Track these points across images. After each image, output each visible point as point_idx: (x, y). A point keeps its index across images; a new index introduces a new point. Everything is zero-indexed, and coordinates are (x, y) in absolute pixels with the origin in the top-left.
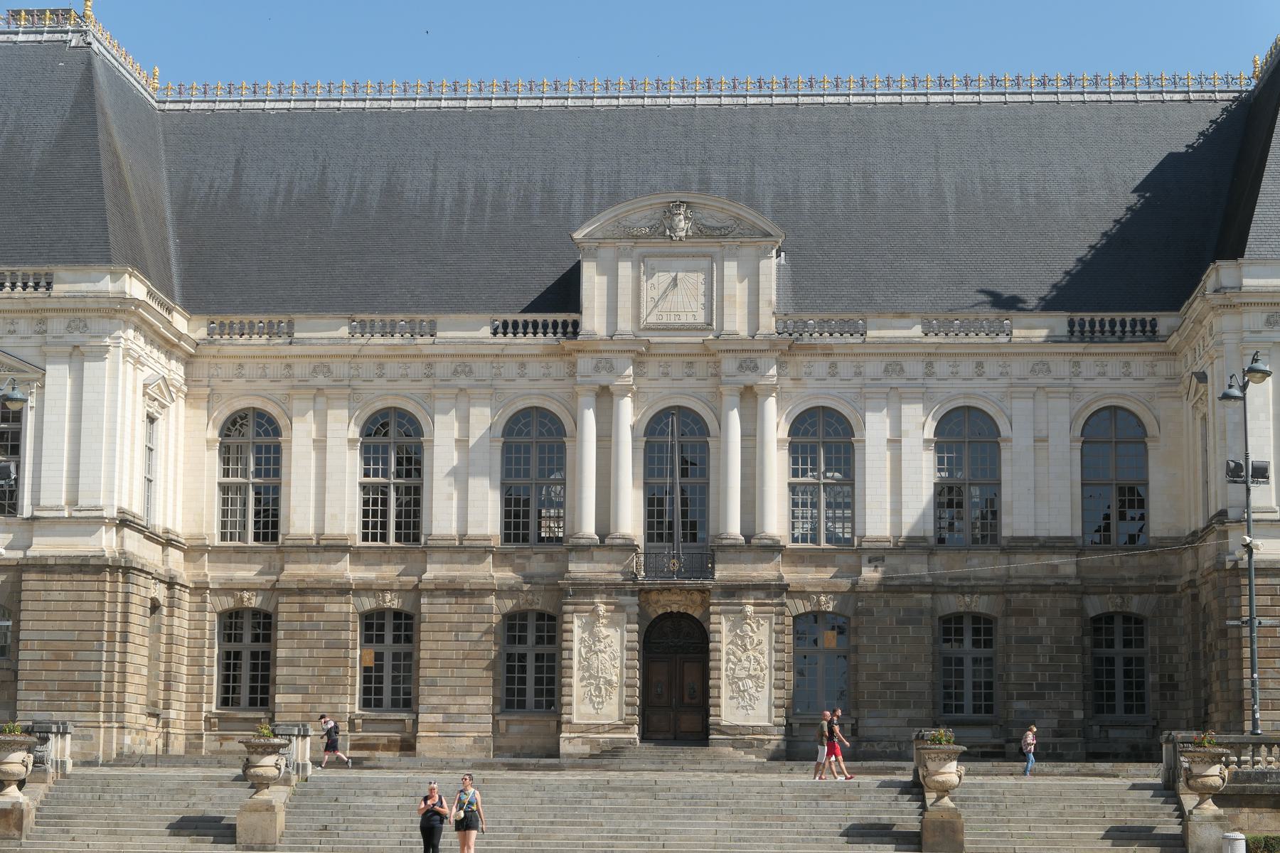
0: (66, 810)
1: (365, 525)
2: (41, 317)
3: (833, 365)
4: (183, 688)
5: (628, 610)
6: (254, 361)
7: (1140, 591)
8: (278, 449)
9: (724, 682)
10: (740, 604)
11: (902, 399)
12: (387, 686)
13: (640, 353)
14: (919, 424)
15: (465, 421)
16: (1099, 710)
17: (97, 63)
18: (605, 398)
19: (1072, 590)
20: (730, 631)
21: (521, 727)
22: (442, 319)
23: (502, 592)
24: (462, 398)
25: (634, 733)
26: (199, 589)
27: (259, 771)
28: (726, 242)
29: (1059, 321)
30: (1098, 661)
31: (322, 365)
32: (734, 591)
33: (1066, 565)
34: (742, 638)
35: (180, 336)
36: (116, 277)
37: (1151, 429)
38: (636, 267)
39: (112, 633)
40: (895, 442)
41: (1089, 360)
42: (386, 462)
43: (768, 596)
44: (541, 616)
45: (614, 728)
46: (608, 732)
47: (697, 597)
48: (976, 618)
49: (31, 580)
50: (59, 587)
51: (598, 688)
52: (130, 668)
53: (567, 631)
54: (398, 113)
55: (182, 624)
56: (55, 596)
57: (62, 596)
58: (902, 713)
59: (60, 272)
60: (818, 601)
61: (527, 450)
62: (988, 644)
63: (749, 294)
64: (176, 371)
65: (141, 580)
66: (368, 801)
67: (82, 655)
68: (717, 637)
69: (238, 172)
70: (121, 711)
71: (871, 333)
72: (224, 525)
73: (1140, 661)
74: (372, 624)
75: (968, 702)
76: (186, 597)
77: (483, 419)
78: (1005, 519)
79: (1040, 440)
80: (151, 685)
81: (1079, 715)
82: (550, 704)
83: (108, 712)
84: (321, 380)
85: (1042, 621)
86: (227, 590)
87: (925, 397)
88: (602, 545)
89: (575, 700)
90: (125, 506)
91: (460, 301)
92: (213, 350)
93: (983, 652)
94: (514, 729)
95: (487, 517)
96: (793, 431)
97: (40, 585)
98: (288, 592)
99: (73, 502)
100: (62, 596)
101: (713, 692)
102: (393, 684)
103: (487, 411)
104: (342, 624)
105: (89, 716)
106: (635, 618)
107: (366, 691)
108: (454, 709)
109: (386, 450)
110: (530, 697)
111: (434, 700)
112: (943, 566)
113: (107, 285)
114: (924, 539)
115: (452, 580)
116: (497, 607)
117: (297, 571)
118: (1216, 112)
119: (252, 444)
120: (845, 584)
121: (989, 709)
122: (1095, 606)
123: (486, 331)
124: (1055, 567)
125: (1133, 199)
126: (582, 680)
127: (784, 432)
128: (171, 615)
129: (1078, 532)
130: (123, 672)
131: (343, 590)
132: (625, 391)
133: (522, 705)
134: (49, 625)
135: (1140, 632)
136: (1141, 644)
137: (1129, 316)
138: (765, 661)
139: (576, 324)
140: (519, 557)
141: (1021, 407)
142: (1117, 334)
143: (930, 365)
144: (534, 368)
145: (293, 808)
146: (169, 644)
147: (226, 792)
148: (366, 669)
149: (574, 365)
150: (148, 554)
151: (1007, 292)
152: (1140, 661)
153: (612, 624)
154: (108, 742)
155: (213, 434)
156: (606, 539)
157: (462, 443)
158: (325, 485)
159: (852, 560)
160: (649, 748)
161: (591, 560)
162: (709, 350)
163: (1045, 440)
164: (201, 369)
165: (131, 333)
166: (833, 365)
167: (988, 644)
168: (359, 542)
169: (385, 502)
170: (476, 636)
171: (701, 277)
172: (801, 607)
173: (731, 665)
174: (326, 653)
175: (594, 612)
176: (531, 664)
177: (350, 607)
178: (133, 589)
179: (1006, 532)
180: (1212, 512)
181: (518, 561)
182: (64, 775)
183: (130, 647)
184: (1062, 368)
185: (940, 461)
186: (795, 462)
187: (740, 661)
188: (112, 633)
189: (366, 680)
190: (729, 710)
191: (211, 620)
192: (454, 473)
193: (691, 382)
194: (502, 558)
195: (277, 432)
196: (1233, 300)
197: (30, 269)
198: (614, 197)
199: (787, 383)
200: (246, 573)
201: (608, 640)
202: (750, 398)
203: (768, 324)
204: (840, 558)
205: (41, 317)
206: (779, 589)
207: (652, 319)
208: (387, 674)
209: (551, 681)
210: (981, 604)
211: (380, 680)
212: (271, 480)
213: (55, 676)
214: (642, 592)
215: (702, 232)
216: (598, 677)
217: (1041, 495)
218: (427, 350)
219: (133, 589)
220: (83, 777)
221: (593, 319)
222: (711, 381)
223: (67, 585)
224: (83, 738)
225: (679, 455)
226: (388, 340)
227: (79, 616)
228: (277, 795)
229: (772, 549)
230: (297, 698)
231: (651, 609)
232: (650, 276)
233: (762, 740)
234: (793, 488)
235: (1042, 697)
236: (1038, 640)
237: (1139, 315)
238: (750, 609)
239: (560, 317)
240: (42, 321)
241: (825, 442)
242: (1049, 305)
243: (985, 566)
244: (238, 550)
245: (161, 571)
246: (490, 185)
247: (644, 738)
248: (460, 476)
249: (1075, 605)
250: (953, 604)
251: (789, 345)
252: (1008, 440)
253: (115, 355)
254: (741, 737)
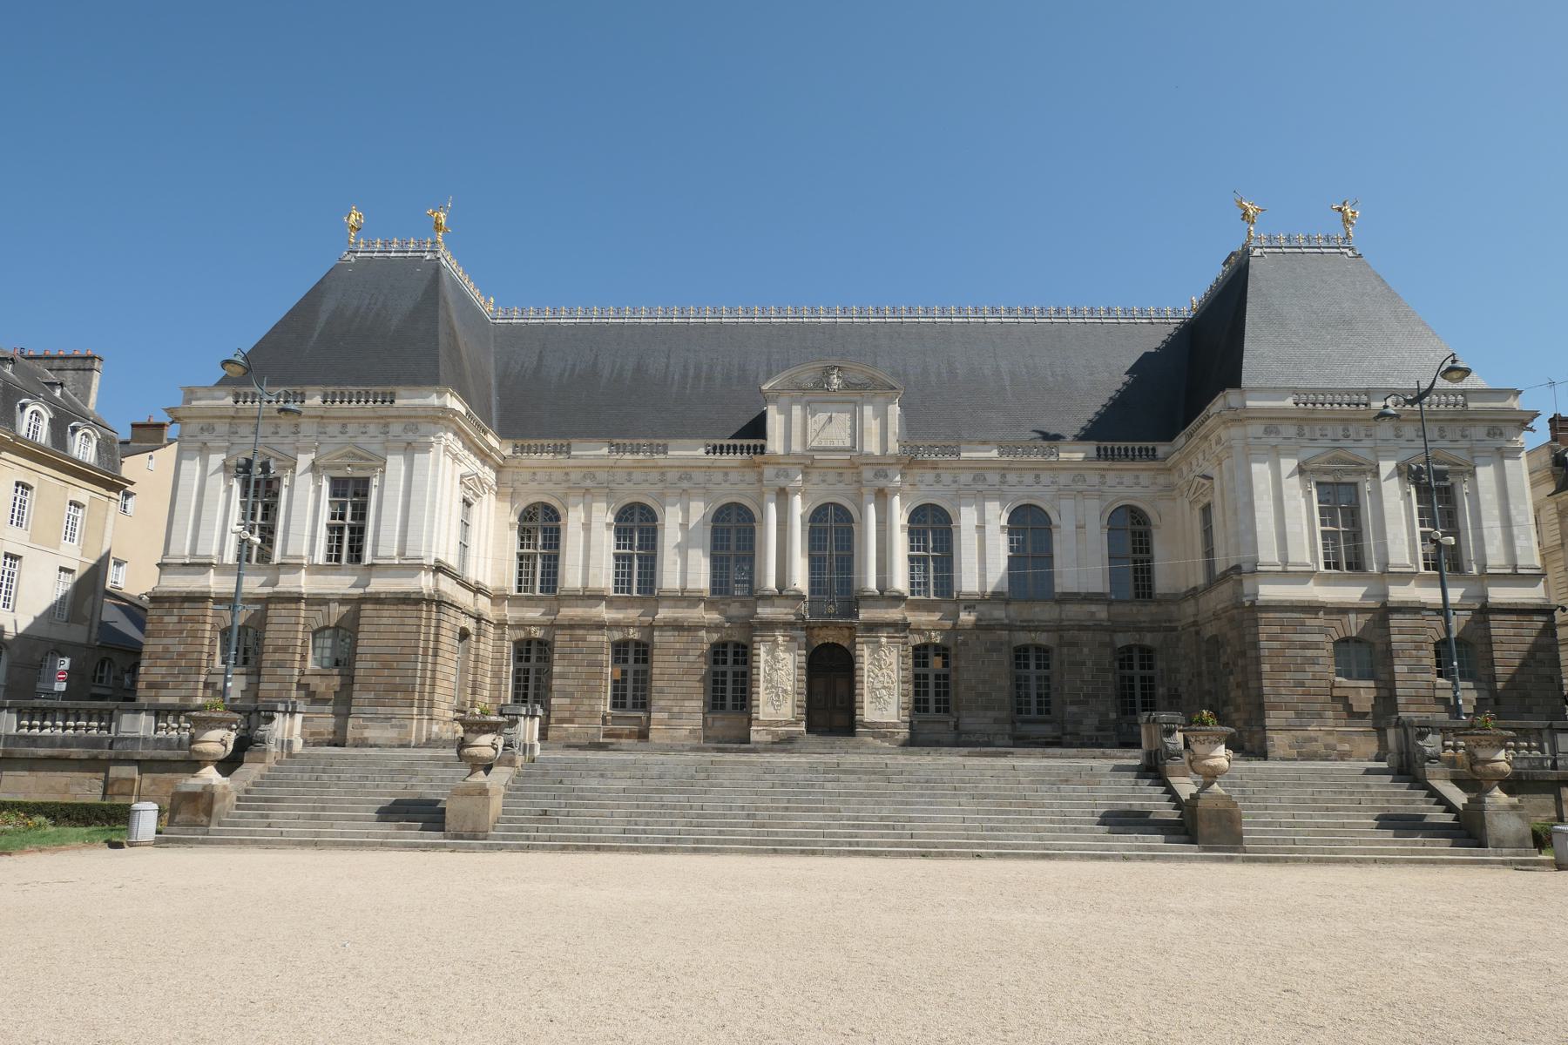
0: (276, 792)
1: (617, 582)
2: (385, 422)
3: (938, 476)
4: (486, 693)
6: (543, 470)
7: (1152, 630)
8: (558, 530)
9: (866, 691)
11: (985, 499)
12: (630, 693)
13: (808, 463)
14: (997, 515)
15: (686, 511)
16: (1125, 713)
17: (444, 272)
18: (783, 496)
19: (1105, 629)
21: (721, 722)
22: (671, 443)
23: (710, 628)
24: (685, 496)
25: (802, 728)
26: (501, 625)
27: (474, 751)
28: (865, 393)
29: (1091, 447)
30: (1123, 678)
31: (589, 472)
32: (873, 627)
33: (1101, 612)
35: (492, 449)
36: (440, 395)
37: (1154, 519)
38: (804, 410)
39: (426, 649)
40: (981, 528)
41: (1111, 474)
42: (632, 539)
44: (737, 645)
45: (789, 723)
47: (846, 632)
48: (1038, 648)
49: (367, 610)
50: (388, 614)
52: (439, 675)
54: (645, 326)
55: (487, 648)
56: (384, 621)
57: (390, 621)
58: (990, 714)
59: (400, 390)
61: (729, 531)
62: (1047, 667)
63: (879, 429)
64: (490, 475)
65: (452, 612)
66: (594, 783)
67: (402, 665)
69: (540, 358)
70: (431, 707)
71: (964, 455)
72: (520, 581)
73: (1151, 679)
74: (620, 649)
75: (1034, 706)
76: (491, 629)
77: (699, 510)
78: (1057, 581)
79: (1080, 527)
80: (462, 690)
81: (1113, 716)
82: (743, 707)
83: (420, 707)
84: (588, 483)
85: (1086, 650)
86: (520, 625)
87: (1001, 497)
88: (780, 595)
90: (442, 558)
91: (684, 430)
92: (516, 462)
93: (1043, 672)
94: (718, 724)
95: (700, 575)
96: (911, 520)
97: (374, 613)
98: (562, 627)
99: (402, 554)
100: (390, 621)
101: (858, 698)
102: (634, 694)
103: (702, 504)
104: (599, 649)
105: (406, 711)
107: (615, 697)
108: (676, 710)
109: (632, 531)
110: (729, 702)
111: (662, 703)
112: (1015, 612)
113: (434, 400)
114: (1002, 593)
115: (676, 620)
116: (707, 638)
117: (568, 613)
118: (1171, 329)
119: (540, 527)
120: (948, 624)
121: (1048, 712)
122: (1121, 640)
123: (701, 451)
124: (1093, 614)
125: (1126, 378)
127: (905, 517)
128: (478, 641)
129: (1107, 590)
130: (433, 678)
131: (600, 626)
132: (796, 491)
133: (723, 707)
134: (379, 643)
135: (1150, 658)
136: (1151, 667)
137: (1137, 445)
138: (894, 676)
139: (763, 447)
141: (1067, 504)
142: (1127, 455)
143: (1004, 476)
144: (734, 476)
145: (514, 791)
146: (476, 661)
147: (450, 773)
148: (616, 682)
149: (761, 474)
150: (464, 597)
151: (1052, 432)
152: (1151, 679)
153: (787, 650)
154: (419, 729)
155: (514, 519)
156: (783, 592)
157: (684, 526)
158: (589, 552)
159: (952, 607)
160: (813, 738)
161: (773, 606)
162: (854, 464)
163: (1083, 527)
164: (507, 476)
165: (450, 436)
166: (938, 476)
167: (1047, 667)
168: (612, 593)
169: (631, 566)
170: (692, 658)
171: (848, 416)
172: (917, 640)
174: (587, 669)
175: (775, 641)
176: (729, 678)
177: (605, 638)
178: (442, 616)
179: (1058, 590)
180: (1220, 568)
182: (290, 755)
183: (440, 660)
184: (1093, 478)
185: (1011, 541)
186: (912, 541)
188: (426, 649)
189: (615, 689)
190: (869, 711)
191: (508, 646)
192: (678, 546)
193: (841, 486)
194: (711, 605)
195: (558, 519)
196: (1241, 417)
197: (379, 389)
198: (787, 367)
199: (907, 487)
200: (534, 614)
202: (882, 496)
203: (894, 447)
204: (944, 606)
205: (385, 422)
206: (903, 627)
207: (815, 444)
208: (630, 685)
209: (743, 691)
210: (1042, 639)
211: (625, 689)
212: (553, 551)
213: (381, 680)
214: (809, 628)
215: (848, 386)
217: (1082, 563)
218: (661, 463)
219: (442, 616)
220: (309, 757)
221: (775, 442)
222: (855, 486)
223: (394, 613)
224: (401, 726)
225: (833, 533)
226: (636, 457)
227: (401, 636)
228: (498, 779)
229: (899, 599)
230: (567, 701)
232: (813, 415)
234: (911, 559)
235: (1086, 703)
236: (1084, 663)
237: (1144, 444)
238: (884, 640)
239: (752, 442)
240: (386, 425)
241: (933, 530)
242: (1086, 436)
243: (1044, 612)
244: (528, 598)
245: (472, 609)
246: (705, 367)
247: (808, 731)
248: (683, 549)
249: (1108, 639)
250: (1023, 638)
251: (909, 462)
252: (1058, 527)
253: (437, 450)
254: (878, 730)
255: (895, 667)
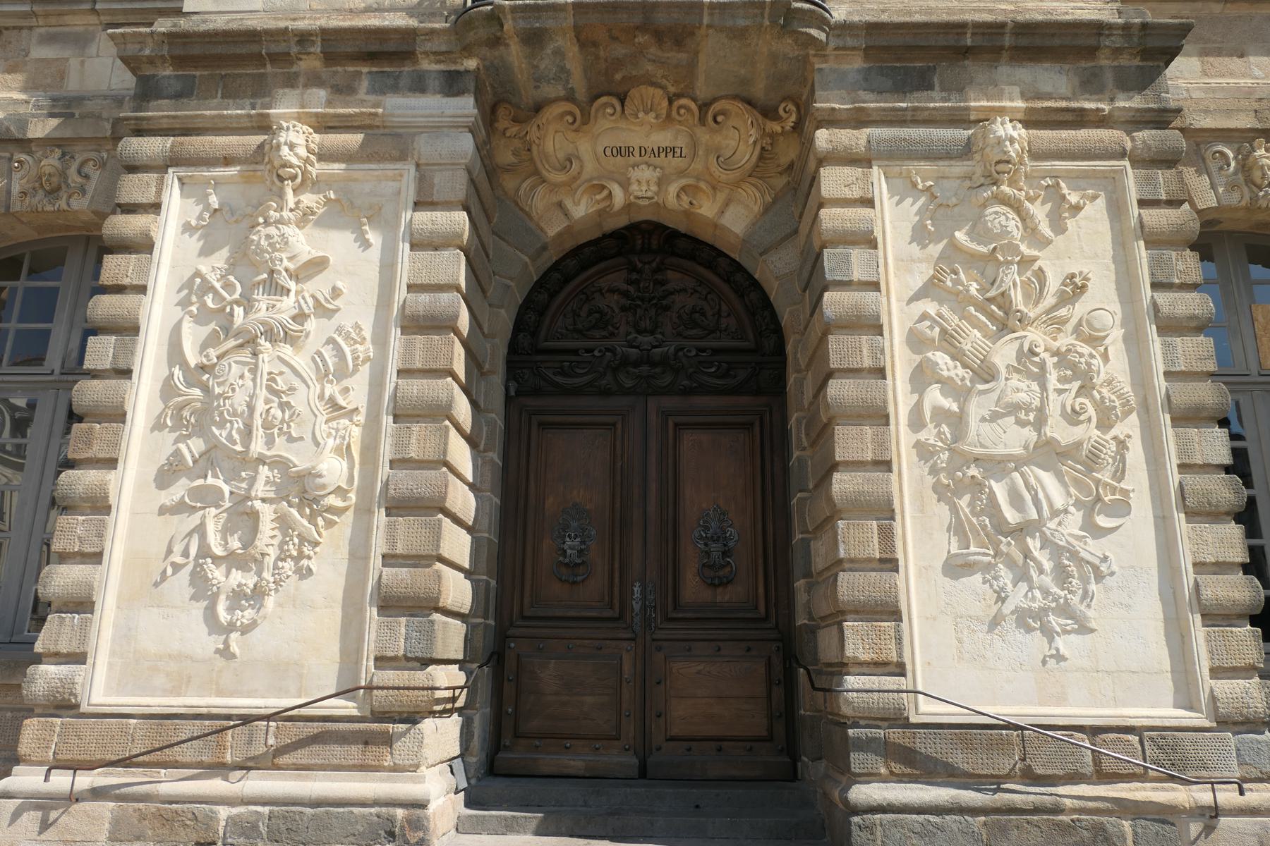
5: (424, 147)
9: (909, 484)
10: (958, 119)
20: (920, 236)
34: (987, 265)
43: (1091, 84)
46: (269, 762)
47: (740, 138)
51: (243, 518)
53: (125, 247)
60: (1246, 167)
68: (857, 263)
89: (112, 583)
106: (457, 185)
126: (167, 475)
138: (1114, 368)
140: (50, 39)
153: (347, 211)
173: (935, 396)
175: (264, 167)
181: (41, 52)
187: (986, 373)
201: (318, 286)
216: (245, 463)
231: (539, 202)
233: (1164, 815)
255: (1102, 302)
